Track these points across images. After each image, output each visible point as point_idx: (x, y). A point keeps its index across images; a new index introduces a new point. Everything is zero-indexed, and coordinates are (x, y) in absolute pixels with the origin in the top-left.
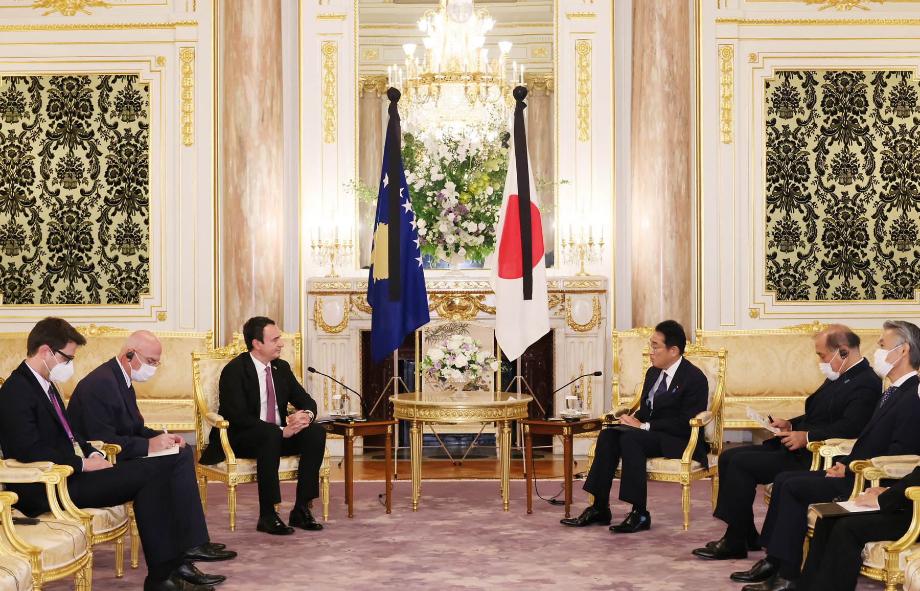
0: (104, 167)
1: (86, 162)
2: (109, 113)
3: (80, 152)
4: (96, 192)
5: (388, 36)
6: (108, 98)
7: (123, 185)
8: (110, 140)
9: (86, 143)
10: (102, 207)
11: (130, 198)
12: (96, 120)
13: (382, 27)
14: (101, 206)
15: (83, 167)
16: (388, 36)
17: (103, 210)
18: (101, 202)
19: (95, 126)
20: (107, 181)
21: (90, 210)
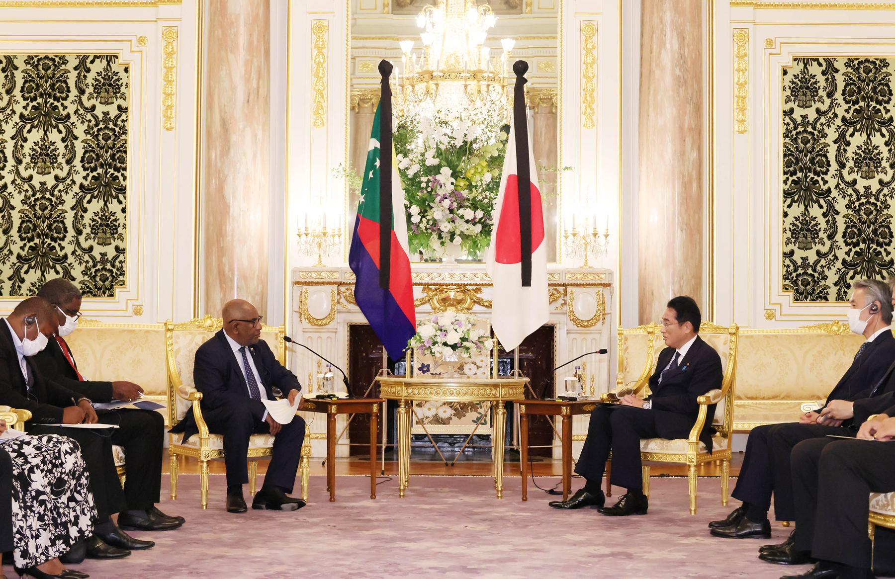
0: (80, 152)
1: (61, 146)
2: (87, 95)
3: (54, 136)
4: (71, 178)
5: (385, 48)
6: (85, 79)
7: (100, 171)
8: (87, 123)
9: (61, 127)
10: (77, 194)
11: (107, 185)
12: (73, 103)
13: (380, 38)
14: (76, 193)
15: (58, 151)
16: (385, 48)
17: (78, 197)
18: (76, 189)
19: (71, 109)
20: (83, 166)
21: (64, 197)
